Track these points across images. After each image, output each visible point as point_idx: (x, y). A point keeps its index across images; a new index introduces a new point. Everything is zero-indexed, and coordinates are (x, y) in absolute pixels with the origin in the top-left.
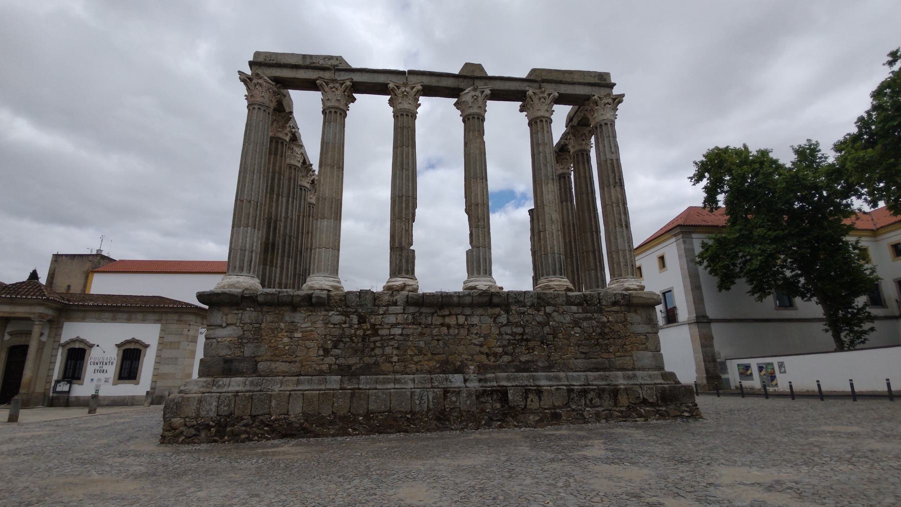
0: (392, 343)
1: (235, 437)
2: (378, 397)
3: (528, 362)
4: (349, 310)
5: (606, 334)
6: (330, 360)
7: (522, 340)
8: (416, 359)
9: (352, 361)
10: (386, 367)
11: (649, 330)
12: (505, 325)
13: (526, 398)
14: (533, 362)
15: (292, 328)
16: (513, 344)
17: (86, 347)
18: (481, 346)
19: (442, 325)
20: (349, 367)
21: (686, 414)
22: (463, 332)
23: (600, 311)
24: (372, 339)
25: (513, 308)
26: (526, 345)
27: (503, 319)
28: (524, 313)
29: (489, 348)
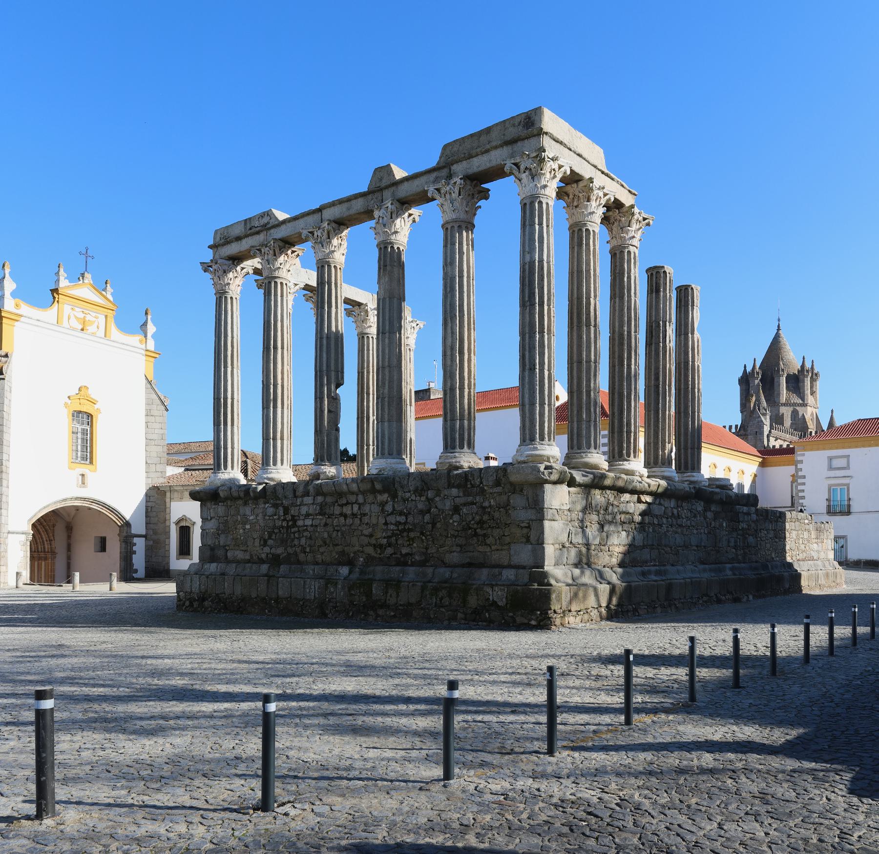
0: (305, 534)
3: (407, 554)
4: (278, 502)
5: (484, 522)
6: (267, 549)
7: (404, 530)
8: (322, 550)
9: (280, 551)
10: (302, 557)
11: (534, 517)
12: (392, 513)
13: (387, 593)
14: (411, 555)
18: (371, 536)
19: (341, 514)
20: (279, 556)
21: (533, 623)
22: (357, 521)
24: (293, 530)
26: (408, 536)
27: (389, 508)
28: (408, 500)
29: (376, 539)
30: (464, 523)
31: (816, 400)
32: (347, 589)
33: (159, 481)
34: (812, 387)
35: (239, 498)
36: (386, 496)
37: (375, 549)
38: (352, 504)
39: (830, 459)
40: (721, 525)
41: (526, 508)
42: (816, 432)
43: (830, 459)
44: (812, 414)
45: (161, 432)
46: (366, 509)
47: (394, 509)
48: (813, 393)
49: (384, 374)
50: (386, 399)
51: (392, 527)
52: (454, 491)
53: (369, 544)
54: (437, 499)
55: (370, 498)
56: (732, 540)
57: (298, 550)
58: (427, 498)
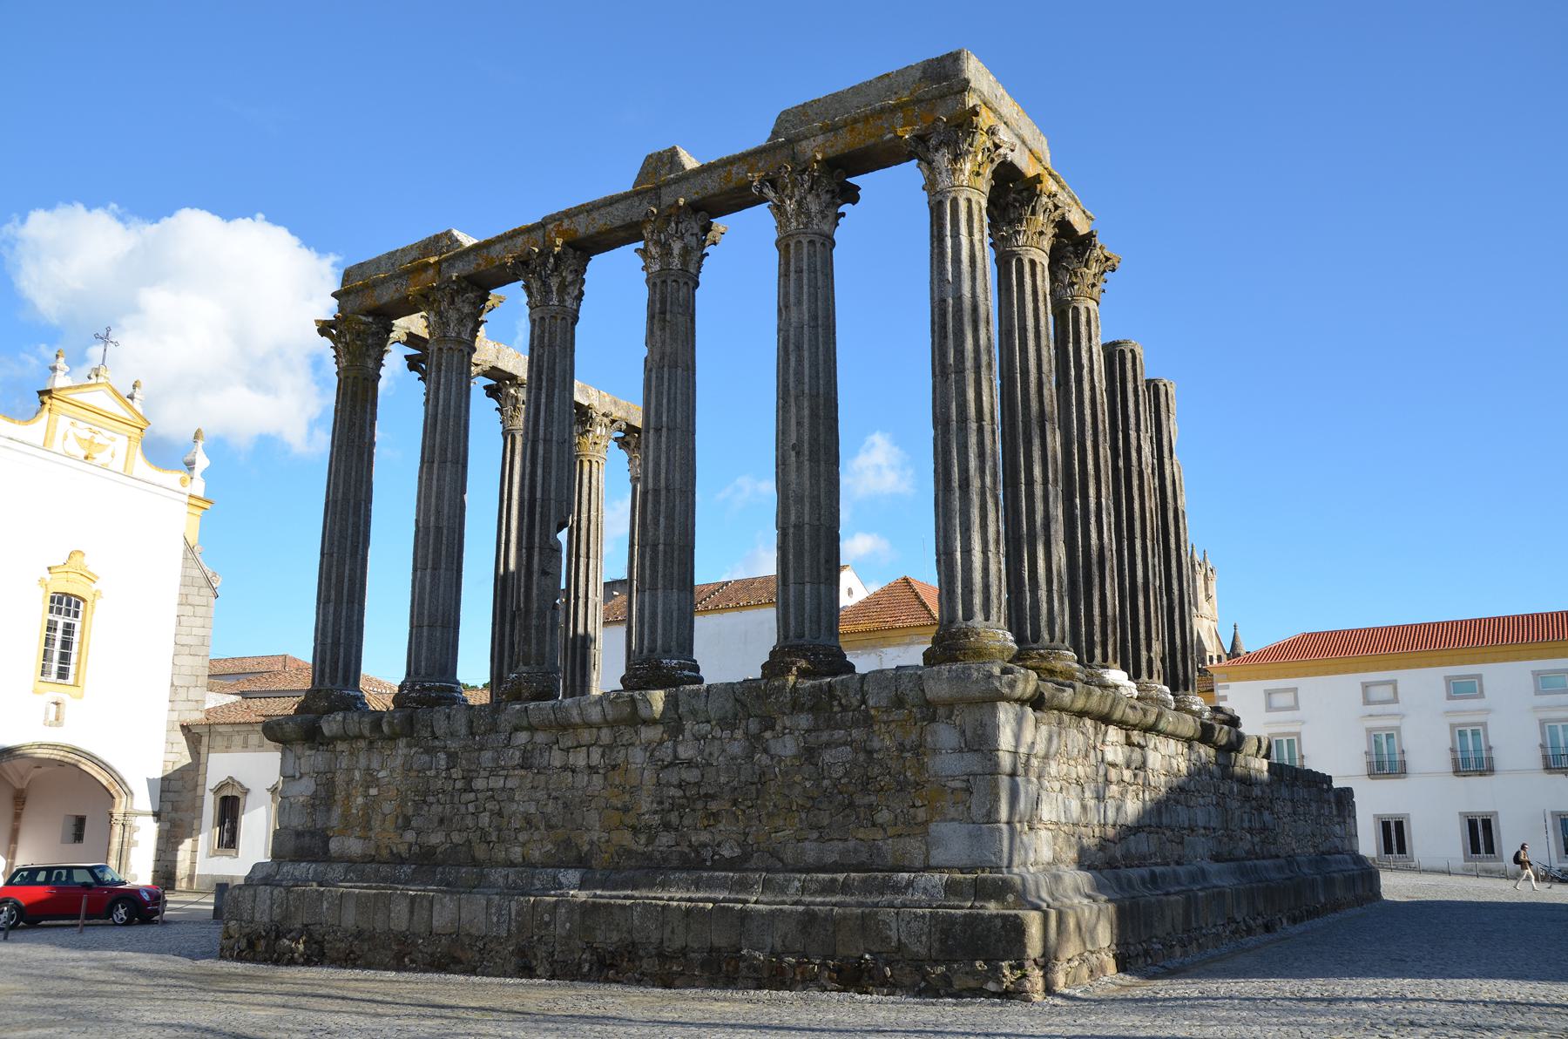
2: (443, 906)
3: (705, 845)
6: (410, 836)
8: (522, 837)
9: (436, 839)
10: (480, 852)
11: (977, 769)
12: (671, 764)
15: (370, 779)
16: (683, 806)
19: (564, 768)
20: (434, 847)
22: (597, 780)
23: (868, 721)
25: (688, 725)
27: (666, 753)
28: (704, 738)
30: (826, 782)
32: (577, 917)
33: (195, 717)
36: (660, 728)
37: (635, 835)
38: (588, 747)
39: (1269, 694)
40: (1231, 790)
41: (961, 751)
42: (1219, 658)
43: (1269, 694)
45: (201, 632)
46: (620, 756)
48: (1208, 597)
49: (657, 502)
50: (661, 547)
51: (673, 792)
52: (804, 721)
53: (622, 825)
54: (768, 735)
55: (627, 735)
56: (1246, 817)
57: (475, 837)
58: (746, 733)
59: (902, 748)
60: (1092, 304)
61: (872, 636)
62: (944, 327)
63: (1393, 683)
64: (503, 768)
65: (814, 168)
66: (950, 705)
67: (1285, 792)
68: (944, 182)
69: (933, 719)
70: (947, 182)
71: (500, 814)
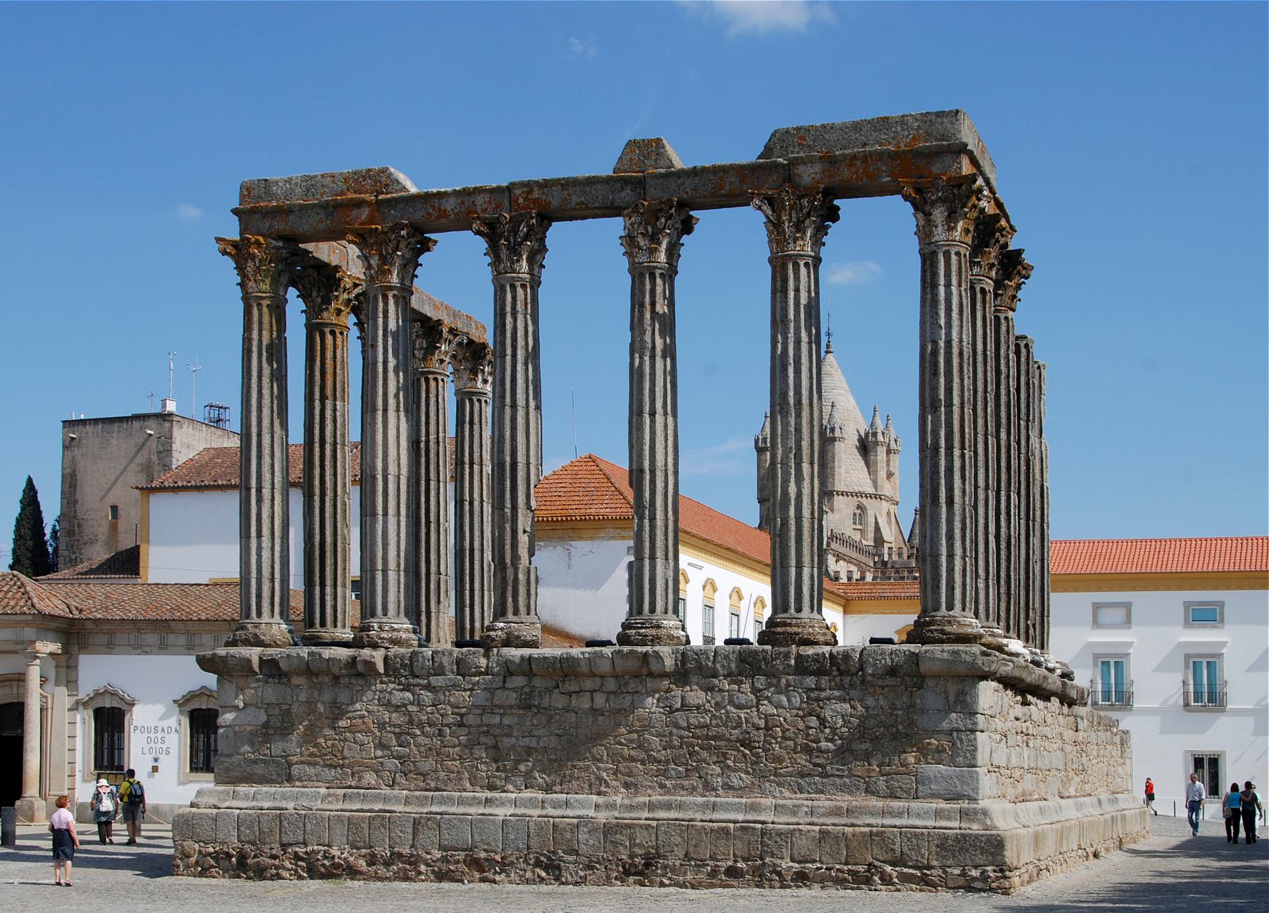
1: (260, 873)
12: (677, 710)
17: (124, 707)
19: (567, 710)
21: (978, 885)
30: (827, 731)
31: (894, 489)
34: (888, 465)
35: (328, 672)
38: (592, 691)
44: (889, 514)
47: (682, 705)
52: (810, 681)
55: (632, 686)
59: (893, 707)
60: (1010, 314)
61: (558, 526)
62: (935, 365)
63: (1128, 606)
64: (499, 707)
65: (800, 188)
66: (937, 677)
67: (1093, 738)
68: (940, 234)
69: (920, 687)
70: (943, 237)
71: (496, 747)
